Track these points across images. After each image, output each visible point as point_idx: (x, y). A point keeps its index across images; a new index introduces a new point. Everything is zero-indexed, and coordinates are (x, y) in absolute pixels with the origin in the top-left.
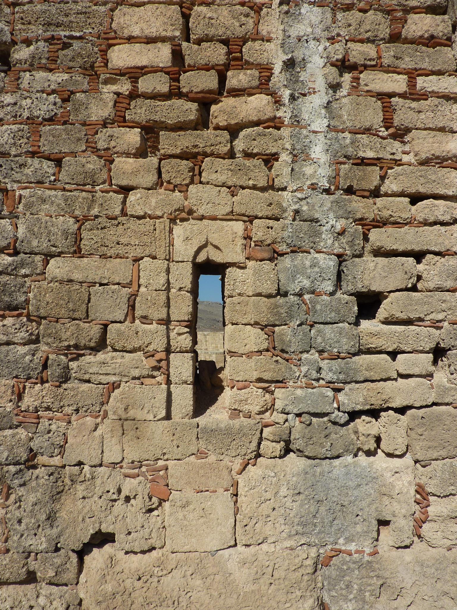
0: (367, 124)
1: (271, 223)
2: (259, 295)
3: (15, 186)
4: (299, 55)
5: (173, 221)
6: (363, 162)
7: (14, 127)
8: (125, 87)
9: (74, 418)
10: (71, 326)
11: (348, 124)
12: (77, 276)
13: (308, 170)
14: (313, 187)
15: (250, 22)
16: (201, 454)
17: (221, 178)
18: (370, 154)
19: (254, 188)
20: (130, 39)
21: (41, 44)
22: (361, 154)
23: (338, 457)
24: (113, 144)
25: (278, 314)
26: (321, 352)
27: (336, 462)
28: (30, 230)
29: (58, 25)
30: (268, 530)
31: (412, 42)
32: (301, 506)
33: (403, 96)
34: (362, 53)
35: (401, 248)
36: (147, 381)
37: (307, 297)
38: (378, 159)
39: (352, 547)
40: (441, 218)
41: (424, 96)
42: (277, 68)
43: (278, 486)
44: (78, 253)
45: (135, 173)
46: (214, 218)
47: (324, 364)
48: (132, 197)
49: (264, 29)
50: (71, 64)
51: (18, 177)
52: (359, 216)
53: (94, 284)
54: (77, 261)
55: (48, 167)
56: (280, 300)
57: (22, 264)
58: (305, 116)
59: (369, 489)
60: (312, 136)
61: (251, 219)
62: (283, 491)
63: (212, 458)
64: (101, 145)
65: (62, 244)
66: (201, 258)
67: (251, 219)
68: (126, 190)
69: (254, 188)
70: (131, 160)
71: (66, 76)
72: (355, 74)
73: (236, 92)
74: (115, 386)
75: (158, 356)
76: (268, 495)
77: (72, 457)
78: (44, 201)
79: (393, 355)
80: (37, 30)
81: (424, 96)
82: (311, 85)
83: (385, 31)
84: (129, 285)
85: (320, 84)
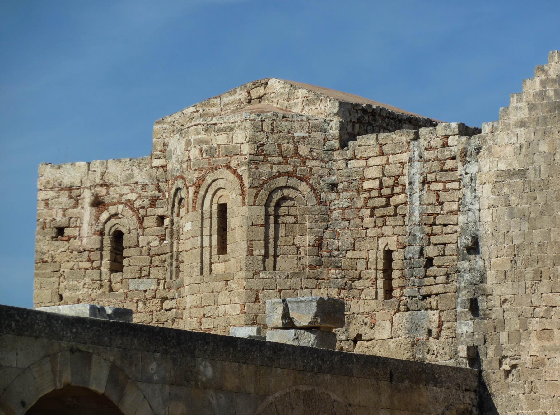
0: (431, 202)
1: (404, 236)
2: (399, 260)
3: (339, 230)
4: (412, 180)
5: (379, 237)
6: (429, 215)
7: (338, 211)
8: (366, 195)
9: (352, 300)
10: (352, 272)
11: (426, 202)
12: (354, 257)
13: (414, 219)
14: (415, 224)
15: (401, 169)
16: (383, 309)
17: (391, 223)
18: (431, 212)
19: (399, 226)
20: (369, 179)
21: (345, 183)
22: (428, 212)
23: (419, 310)
24: (363, 214)
25: (404, 266)
26: (415, 277)
27: (419, 312)
28: (342, 243)
29: (350, 176)
30: (400, 332)
31: (447, 171)
32: (408, 325)
33: (442, 190)
34: (431, 177)
35: (438, 243)
36: (370, 288)
37: (412, 260)
38: (433, 213)
39: (422, 338)
40: (449, 232)
41: (449, 190)
42: (407, 185)
43: (403, 319)
44: (354, 249)
45: (368, 223)
46: (389, 236)
47: (416, 281)
48: (369, 231)
49: (404, 172)
50: (353, 189)
51: (339, 227)
52: (427, 233)
53: (358, 259)
54: (354, 252)
55: (347, 223)
56: (405, 261)
57: (340, 254)
58: (414, 201)
59: (427, 320)
60: (415, 207)
61: (399, 235)
62: (404, 320)
63: (387, 311)
64: (360, 215)
65: (350, 247)
66: (386, 249)
67: (399, 235)
68: (367, 228)
69: (399, 226)
70: (368, 219)
71: (351, 193)
72: (429, 185)
73: (397, 194)
74: (363, 290)
75: (373, 280)
76: (400, 322)
77: (352, 312)
78: (346, 234)
79: (435, 277)
80: (344, 178)
81: (449, 190)
82: (416, 190)
83: (438, 168)
84: (366, 259)
85: (418, 190)
